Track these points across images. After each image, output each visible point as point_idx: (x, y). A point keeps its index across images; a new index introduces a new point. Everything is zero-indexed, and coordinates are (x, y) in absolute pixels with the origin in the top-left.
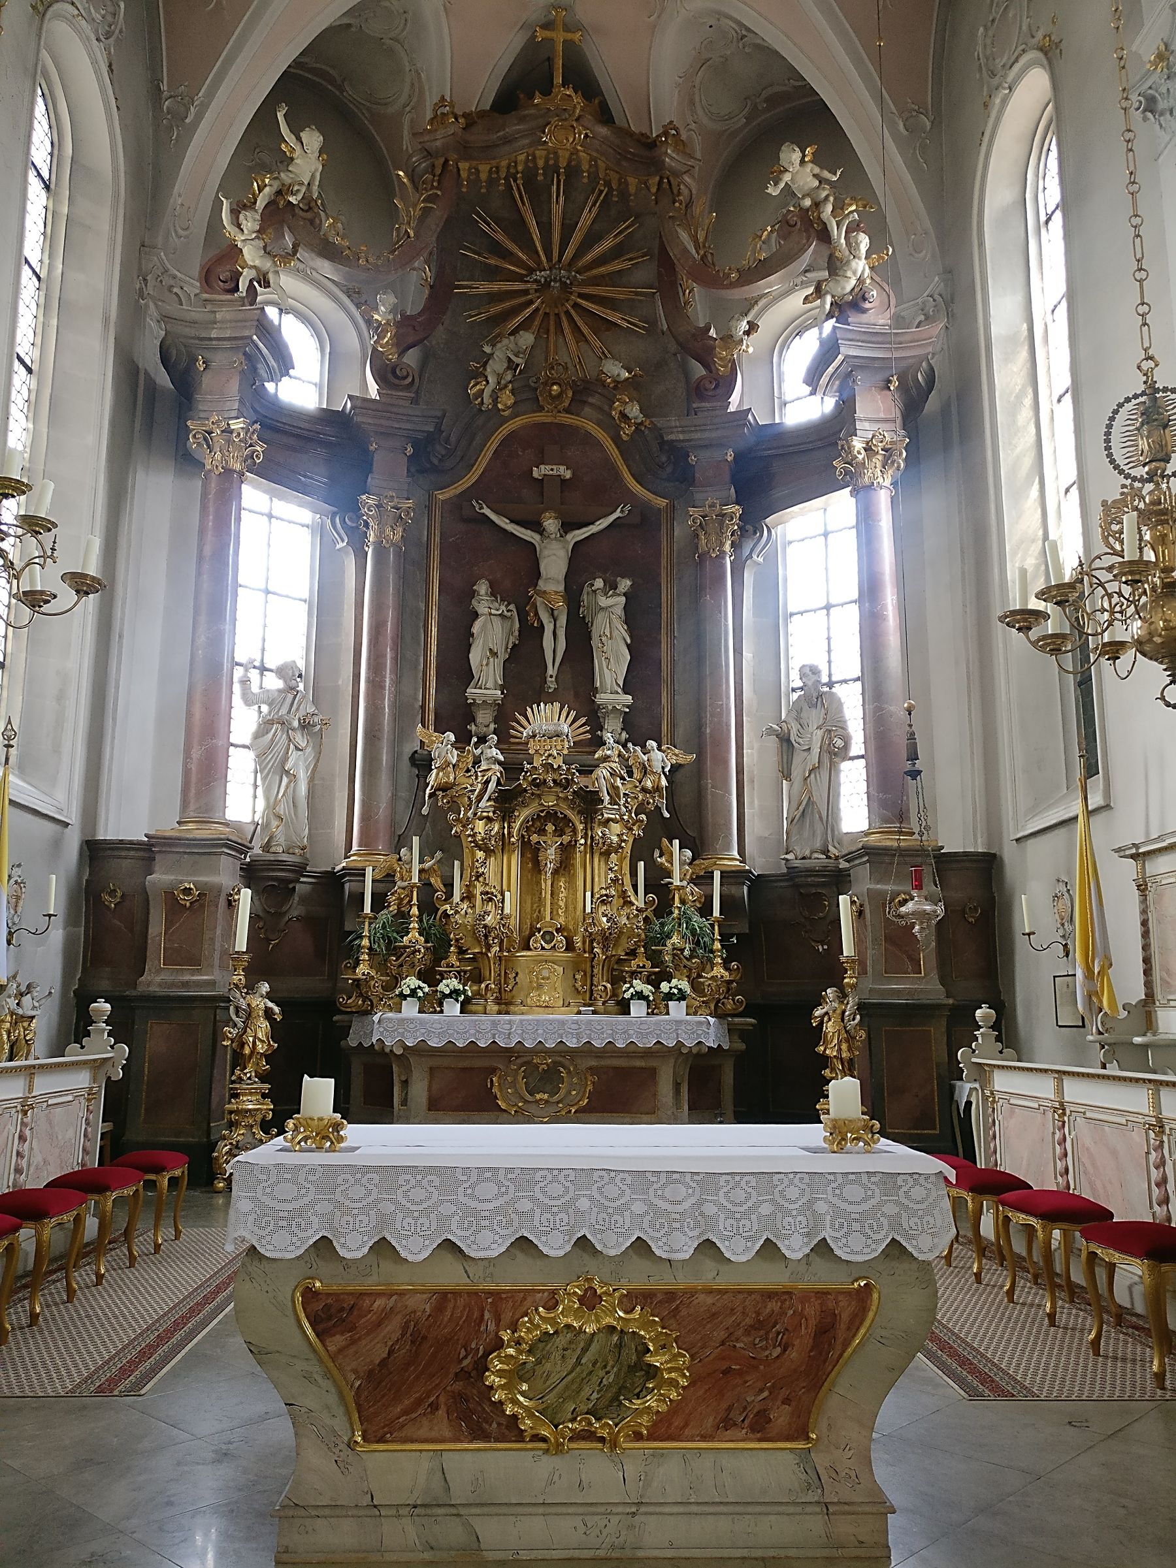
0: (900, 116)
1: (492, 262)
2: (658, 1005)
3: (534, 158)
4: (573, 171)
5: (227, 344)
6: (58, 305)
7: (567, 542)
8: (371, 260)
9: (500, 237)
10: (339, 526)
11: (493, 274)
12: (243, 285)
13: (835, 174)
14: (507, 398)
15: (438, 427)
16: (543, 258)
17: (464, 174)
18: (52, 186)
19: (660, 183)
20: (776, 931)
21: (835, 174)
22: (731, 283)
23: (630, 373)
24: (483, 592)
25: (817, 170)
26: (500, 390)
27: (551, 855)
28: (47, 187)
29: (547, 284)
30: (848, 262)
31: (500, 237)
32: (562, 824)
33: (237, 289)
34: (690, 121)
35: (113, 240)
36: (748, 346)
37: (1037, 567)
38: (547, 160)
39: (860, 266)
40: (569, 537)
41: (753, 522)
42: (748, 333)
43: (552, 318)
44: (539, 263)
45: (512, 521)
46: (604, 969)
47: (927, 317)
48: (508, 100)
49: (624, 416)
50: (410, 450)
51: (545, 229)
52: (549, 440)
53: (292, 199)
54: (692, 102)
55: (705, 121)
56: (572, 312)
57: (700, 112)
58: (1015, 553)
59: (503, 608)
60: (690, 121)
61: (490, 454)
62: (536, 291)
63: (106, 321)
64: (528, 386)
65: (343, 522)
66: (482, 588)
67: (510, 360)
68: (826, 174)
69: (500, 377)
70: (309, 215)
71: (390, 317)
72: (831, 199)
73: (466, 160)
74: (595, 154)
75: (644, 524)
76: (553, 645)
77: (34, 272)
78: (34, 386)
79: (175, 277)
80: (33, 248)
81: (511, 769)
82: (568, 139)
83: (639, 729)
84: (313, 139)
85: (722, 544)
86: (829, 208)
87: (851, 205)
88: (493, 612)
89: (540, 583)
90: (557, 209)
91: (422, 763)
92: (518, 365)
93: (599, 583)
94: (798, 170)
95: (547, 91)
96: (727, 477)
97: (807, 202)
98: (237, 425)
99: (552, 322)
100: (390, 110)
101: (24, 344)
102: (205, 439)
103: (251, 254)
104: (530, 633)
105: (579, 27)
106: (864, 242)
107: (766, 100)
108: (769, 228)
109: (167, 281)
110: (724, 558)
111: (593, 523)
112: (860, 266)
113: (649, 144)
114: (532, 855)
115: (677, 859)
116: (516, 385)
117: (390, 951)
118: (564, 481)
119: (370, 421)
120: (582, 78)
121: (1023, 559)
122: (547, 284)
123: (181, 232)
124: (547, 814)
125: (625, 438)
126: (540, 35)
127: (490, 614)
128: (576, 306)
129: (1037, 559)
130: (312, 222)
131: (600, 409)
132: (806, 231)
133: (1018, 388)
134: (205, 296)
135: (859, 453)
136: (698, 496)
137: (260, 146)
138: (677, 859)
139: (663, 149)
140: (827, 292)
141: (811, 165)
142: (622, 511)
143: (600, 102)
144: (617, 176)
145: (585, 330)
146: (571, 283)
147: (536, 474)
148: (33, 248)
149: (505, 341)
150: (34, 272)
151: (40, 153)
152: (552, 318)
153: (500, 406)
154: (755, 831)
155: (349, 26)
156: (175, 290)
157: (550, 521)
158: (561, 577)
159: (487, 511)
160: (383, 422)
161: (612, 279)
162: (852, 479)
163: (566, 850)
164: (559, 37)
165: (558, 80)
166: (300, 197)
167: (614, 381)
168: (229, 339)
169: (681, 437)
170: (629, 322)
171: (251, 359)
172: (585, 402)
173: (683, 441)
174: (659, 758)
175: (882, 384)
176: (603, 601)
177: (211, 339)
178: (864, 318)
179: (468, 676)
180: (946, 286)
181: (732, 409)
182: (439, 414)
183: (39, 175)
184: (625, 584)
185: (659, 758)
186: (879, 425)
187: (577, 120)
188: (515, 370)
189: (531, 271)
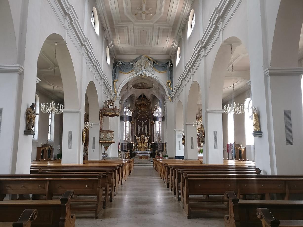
2: (148, 151)
20: (154, 146)
27: (143, 143)
32: (143, 141)
46: (145, 149)
64: (141, 112)
66: (138, 125)
75: (148, 121)
76: (143, 129)
81: (141, 138)
83: (148, 135)
91: (135, 137)
114: (142, 143)
115: (149, 143)
117: (135, 148)
120: (144, 96)
124: (143, 141)
138: (149, 143)
154: (155, 140)
163: (144, 143)
174: (149, 137)
184: (147, 125)
185: (149, 137)
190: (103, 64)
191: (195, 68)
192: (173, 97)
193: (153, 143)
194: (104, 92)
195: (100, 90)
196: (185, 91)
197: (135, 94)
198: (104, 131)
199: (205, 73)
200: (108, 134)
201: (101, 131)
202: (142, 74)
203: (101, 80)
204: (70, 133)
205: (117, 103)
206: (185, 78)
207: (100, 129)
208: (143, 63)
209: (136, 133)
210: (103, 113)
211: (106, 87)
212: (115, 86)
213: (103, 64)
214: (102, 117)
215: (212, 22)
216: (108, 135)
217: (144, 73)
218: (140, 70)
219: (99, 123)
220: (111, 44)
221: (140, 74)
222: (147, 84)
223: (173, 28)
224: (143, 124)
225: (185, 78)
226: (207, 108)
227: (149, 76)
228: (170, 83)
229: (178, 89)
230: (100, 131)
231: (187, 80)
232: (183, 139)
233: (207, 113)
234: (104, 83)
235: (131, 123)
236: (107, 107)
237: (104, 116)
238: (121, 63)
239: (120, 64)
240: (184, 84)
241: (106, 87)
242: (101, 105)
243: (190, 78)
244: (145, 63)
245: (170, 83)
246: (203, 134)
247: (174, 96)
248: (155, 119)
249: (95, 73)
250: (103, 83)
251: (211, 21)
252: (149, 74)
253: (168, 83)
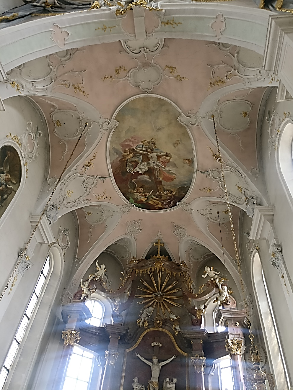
0: (234, 260)
1: (145, 290)
3: (152, 269)
4: (161, 271)
5: (75, 312)
6: (40, 303)
7: (159, 366)
8: (112, 292)
9: (147, 285)
10: (99, 359)
11: (145, 293)
12: (82, 298)
13: (218, 273)
14: (146, 324)
15: (127, 332)
16: (156, 289)
17: (137, 272)
18: (47, 278)
19: (181, 274)
21: (218, 273)
22: (196, 297)
23: (177, 317)
24: (136, 381)
25: (214, 272)
26: (145, 322)
28: (45, 278)
29: (157, 295)
30: (223, 293)
31: (147, 285)
33: (81, 299)
34: (189, 260)
35: (56, 289)
36: (205, 312)
37: (284, 382)
38: (155, 269)
39: (226, 294)
40: (160, 364)
42: (204, 308)
43: (158, 304)
44: (156, 291)
45: (145, 359)
47: (248, 305)
48: (148, 257)
49: (175, 328)
50: (119, 338)
51: (157, 283)
53: (96, 279)
54: (189, 256)
55: (193, 260)
56: (163, 302)
57: (191, 258)
58: (277, 377)
59: (141, 387)
60: (189, 260)
61: (141, 339)
62: (155, 297)
63: (50, 306)
65: (100, 358)
66: (136, 380)
67: (147, 314)
68: (216, 273)
69: (144, 318)
70: (100, 282)
71: (118, 304)
72: (218, 278)
73: (137, 269)
74: (165, 268)
77: (37, 296)
78: (28, 323)
79: (70, 295)
80: (38, 290)
82: (160, 264)
84: (103, 267)
85: (201, 369)
86: (217, 280)
87: (223, 279)
88: (138, 388)
89: (152, 378)
90: (160, 279)
92: (149, 316)
93: (168, 380)
94: (209, 272)
95: (156, 255)
96: (201, 348)
97: (212, 279)
98: (73, 332)
99: (158, 305)
100: (124, 258)
101: (29, 312)
102: (66, 336)
103: (85, 291)
105: (163, 243)
106: (226, 288)
107: (207, 255)
108: (204, 285)
109: (68, 296)
110: (201, 373)
111: (167, 360)
112: (226, 294)
113: (179, 265)
116: (149, 320)
118: (160, 347)
119: (110, 330)
120: (164, 252)
121: (280, 379)
122: (157, 295)
123: (74, 285)
125: (176, 335)
126: (155, 245)
127: (137, 389)
128: (164, 300)
129: (284, 379)
130: (100, 284)
131: (170, 327)
132: (213, 285)
133: (270, 327)
134: (74, 300)
135: (230, 344)
136: (193, 353)
137: (93, 269)
139: (181, 267)
140: (219, 300)
141: (212, 271)
142: (175, 357)
143: (168, 257)
144: (171, 272)
145: (166, 306)
146: (163, 295)
147: (152, 345)
148: (38, 290)
149: (146, 309)
150: (37, 296)
151: (45, 271)
152: (158, 304)
153: (144, 326)
155: (117, 244)
156: (70, 298)
157: (155, 359)
158: (157, 377)
159: (139, 356)
160: (113, 331)
162: (228, 352)
164: (159, 245)
165: (159, 253)
166: (98, 278)
167: (173, 320)
168: (76, 311)
169: (188, 336)
170: (177, 305)
171: (81, 315)
172: (166, 325)
173: (189, 337)
175: (235, 324)
176: (169, 386)
177: (72, 311)
178: (228, 306)
180: (251, 298)
181: (201, 328)
182: (127, 328)
183: (44, 276)
184: (175, 380)
186: (235, 336)
187: (161, 261)
188: (149, 317)
189: (154, 292)
197: (133, 240)
248: (213, 346)
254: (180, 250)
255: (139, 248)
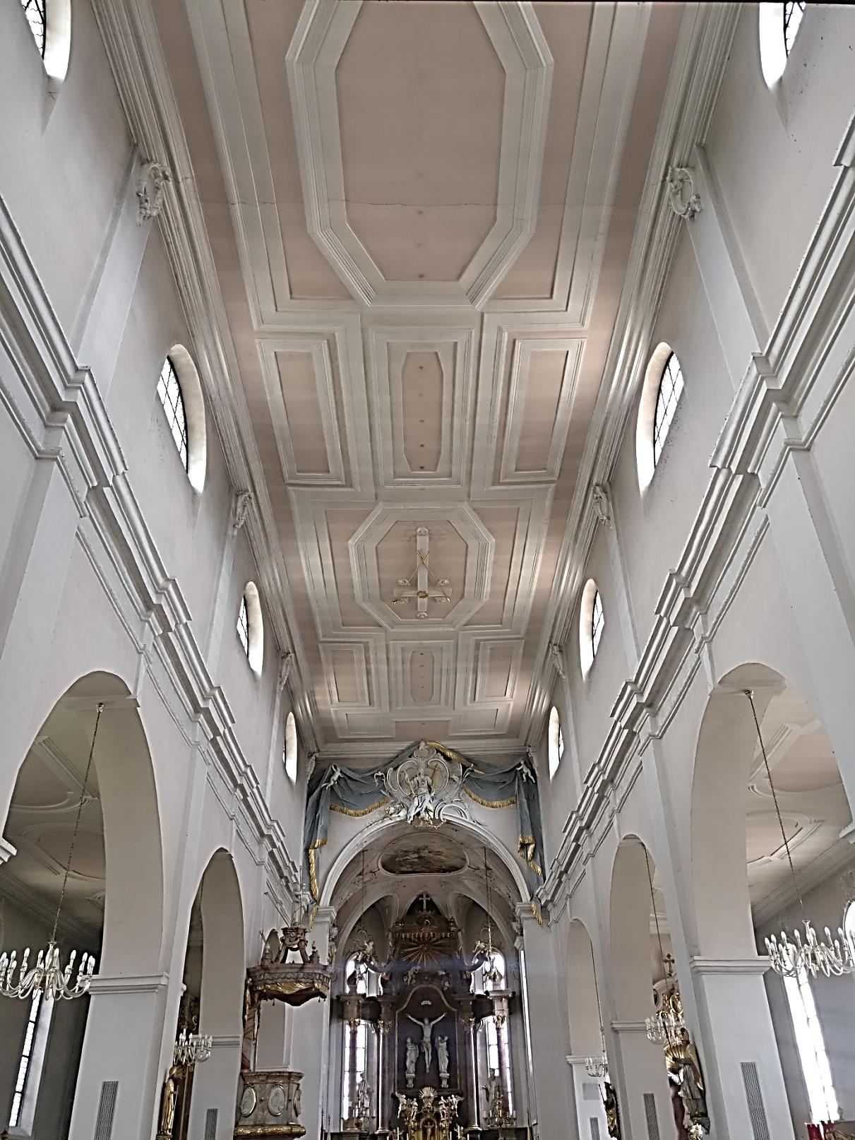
32: (432, 1122)
41: (478, 1021)
52: (425, 994)
76: (428, 1058)
83: (453, 1088)
91: (396, 1101)
104: (422, 1054)
115: (459, 1129)
120: (431, 905)
138: (459, 1129)
161: (440, 945)
174: (455, 1100)
179: (405, 1068)
185: (455, 1100)
190: (269, 781)
191: (624, 785)
192: (550, 907)
193: (477, 1131)
194: (270, 894)
195: (253, 882)
196: (596, 876)
197: (395, 896)
198: (258, 1075)
199: (667, 802)
200: (273, 1092)
201: (247, 1078)
202: (418, 814)
203: (260, 843)
204: (110, 1090)
205: (319, 940)
206: (588, 826)
207: (243, 1067)
208: (421, 771)
209: (399, 1080)
210: (262, 988)
211: (279, 869)
212: (313, 866)
213: (269, 781)
214: (253, 1002)
215: (723, 467)
216: (277, 1097)
217: (427, 810)
218: (410, 798)
219: (241, 1040)
220: (272, 574)
221: (413, 814)
222: (439, 853)
223: (557, 491)
224: (427, 1032)
225: (588, 826)
226: (693, 950)
227: (448, 822)
228: (532, 847)
229: (566, 871)
230: (241, 1074)
231: (598, 834)
232: (609, 1105)
233: (697, 972)
234: (271, 854)
235: (378, 1032)
236: (277, 958)
237: (263, 1002)
238: (338, 774)
239: (335, 777)
240: (585, 850)
241: (279, 869)
242: (252, 949)
243: (611, 824)
244: (431, 771)
245: (532, 847)
246: (696, 1080)
247: (552, 900)
248: (482, 1006)
249: (239, 817)
250: (266, 857)
251: (719, 465)
252: (447, 814)
253: (524, 846)
254: (447, 901)
255: (402, 901)
